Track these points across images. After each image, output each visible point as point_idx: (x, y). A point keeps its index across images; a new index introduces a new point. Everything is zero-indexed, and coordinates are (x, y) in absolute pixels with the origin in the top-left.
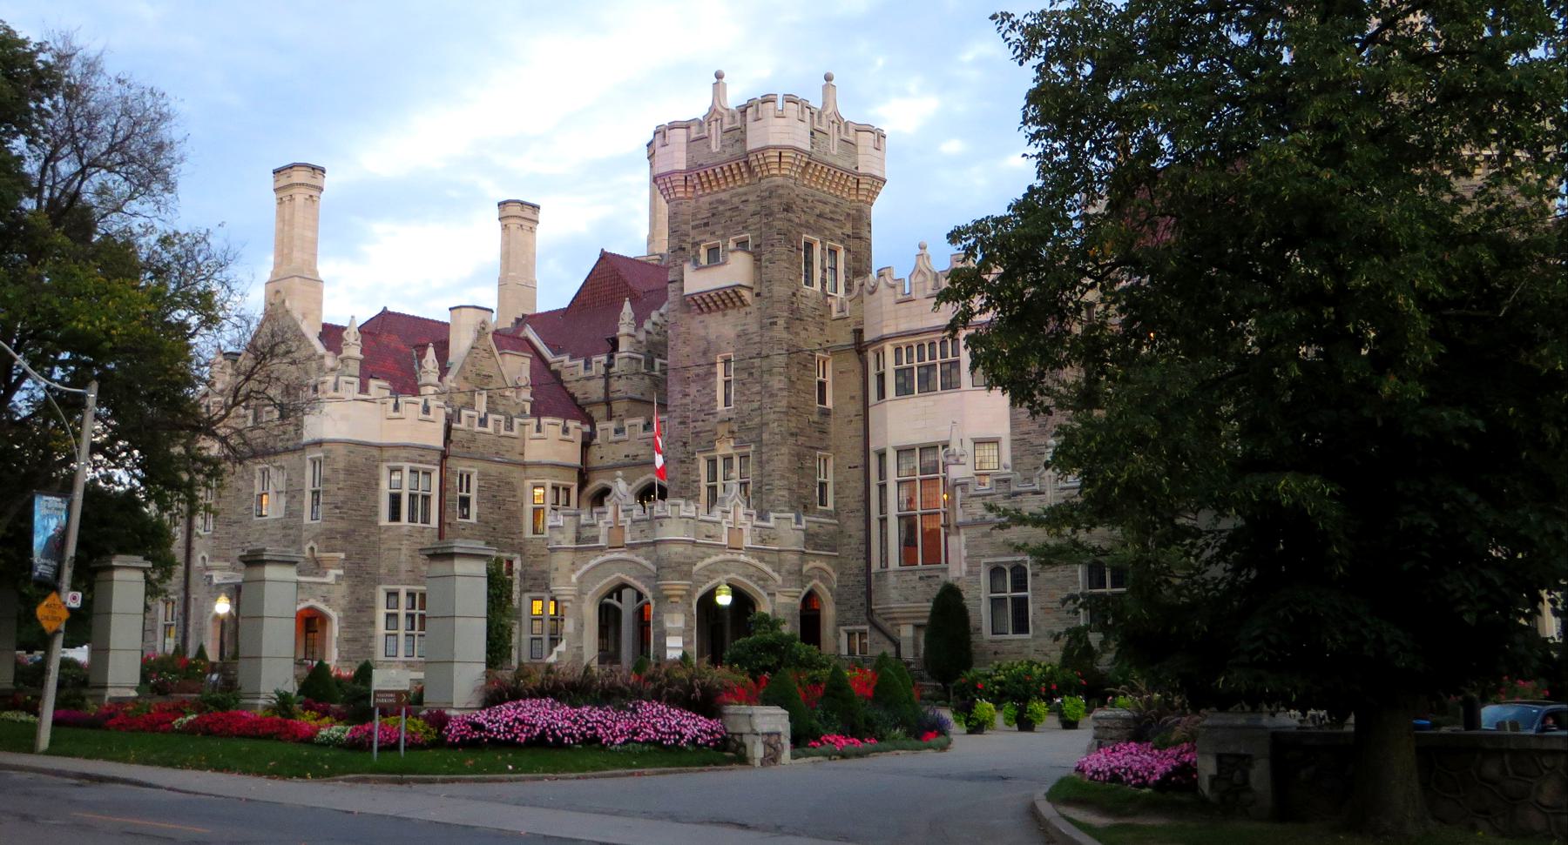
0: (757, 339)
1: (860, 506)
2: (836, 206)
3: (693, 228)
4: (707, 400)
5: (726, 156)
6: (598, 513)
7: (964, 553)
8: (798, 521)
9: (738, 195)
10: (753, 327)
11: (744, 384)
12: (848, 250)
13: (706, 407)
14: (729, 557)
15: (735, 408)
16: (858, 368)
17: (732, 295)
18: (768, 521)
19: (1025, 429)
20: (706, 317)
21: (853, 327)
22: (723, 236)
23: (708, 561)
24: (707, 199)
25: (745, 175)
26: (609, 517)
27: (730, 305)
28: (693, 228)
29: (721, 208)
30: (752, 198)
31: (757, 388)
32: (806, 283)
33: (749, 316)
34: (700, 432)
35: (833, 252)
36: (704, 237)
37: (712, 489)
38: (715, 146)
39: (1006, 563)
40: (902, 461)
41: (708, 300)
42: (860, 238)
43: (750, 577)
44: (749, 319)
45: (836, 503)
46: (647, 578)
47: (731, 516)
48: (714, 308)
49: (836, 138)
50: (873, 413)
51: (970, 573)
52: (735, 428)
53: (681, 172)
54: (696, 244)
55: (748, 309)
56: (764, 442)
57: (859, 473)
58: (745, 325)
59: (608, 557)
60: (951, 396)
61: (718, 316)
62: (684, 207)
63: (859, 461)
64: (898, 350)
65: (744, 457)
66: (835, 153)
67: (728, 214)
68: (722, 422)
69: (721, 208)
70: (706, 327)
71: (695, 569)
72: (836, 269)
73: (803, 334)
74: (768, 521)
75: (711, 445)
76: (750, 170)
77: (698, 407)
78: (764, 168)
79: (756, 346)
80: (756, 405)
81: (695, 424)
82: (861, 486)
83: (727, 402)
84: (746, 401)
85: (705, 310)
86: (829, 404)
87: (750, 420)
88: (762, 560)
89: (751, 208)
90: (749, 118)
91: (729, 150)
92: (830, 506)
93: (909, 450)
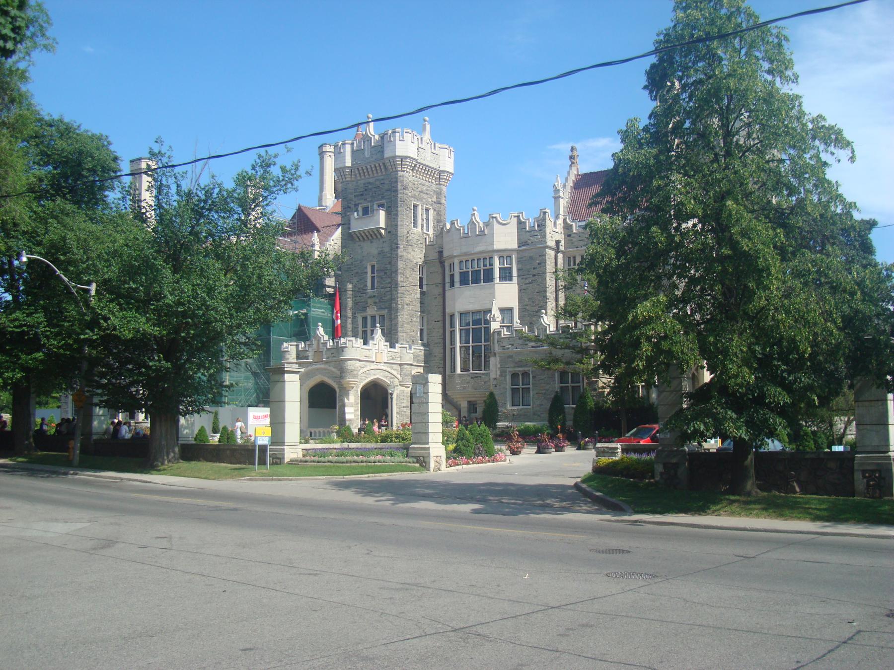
0: (389, 255)
1: (441, 341)
2: (428, 187)
3: (355, 196)
5: (373, 159)
7: (499, 366)
8: (410, 348)
9: (378, 180)
10: (387, 249)
12: (434, 210)
14: (376, 367)
16: (440, 270)
17: (376, 232)
18: (395, 348)
19: (525, 303)
21: (437, 250)
22: (371, 201)
23: (366, 369)
24: (363, 182)
25: (383, 170)
26: (315, 346)
27: (375, 237)
28: (355, 196)
29: (370, 187)
30: (387, 182)
31: (389, 280)
32: (414, 227)
35: (427, 210)
37: (365, 332)
38: (367, 154)
39: (519, 371)
40: (463, 318)
41: (363, 234)
42: (441, 204)
43: (386, 377)
45: (428, 339)
46: (335, 378)
47: (377, 346)
48: (366, 238)
49: (430, 151)
50: (448, 294)
51: (501, 376)
52: (377, 301)
53: (349, 167)
54: (356, 205)
55: (384, 240)
57: (440, 324)
59: (314, 367)
62: (350, 186)
63: (441, 318)
64: (461, 262)
65: (382, 316)
66: (428, 159)
67: (373, 190)
68: (370, 297)
69: (370, 187)
70: (362, 248)
71: (360, 373)
72: (427, 219)
73: (412, 253)
74: (395, 348)
75: (364, 309)
76: (386, 168)
78: (393, 167)
80: (388, 289)
82: (441, 331)
83: (373, 287)
85: (361, 239)
86: (425, 289)
88: (392, 368)
89: (386, 187)
90: (385, 140)
92: (425, 341)
93: (467, 313)
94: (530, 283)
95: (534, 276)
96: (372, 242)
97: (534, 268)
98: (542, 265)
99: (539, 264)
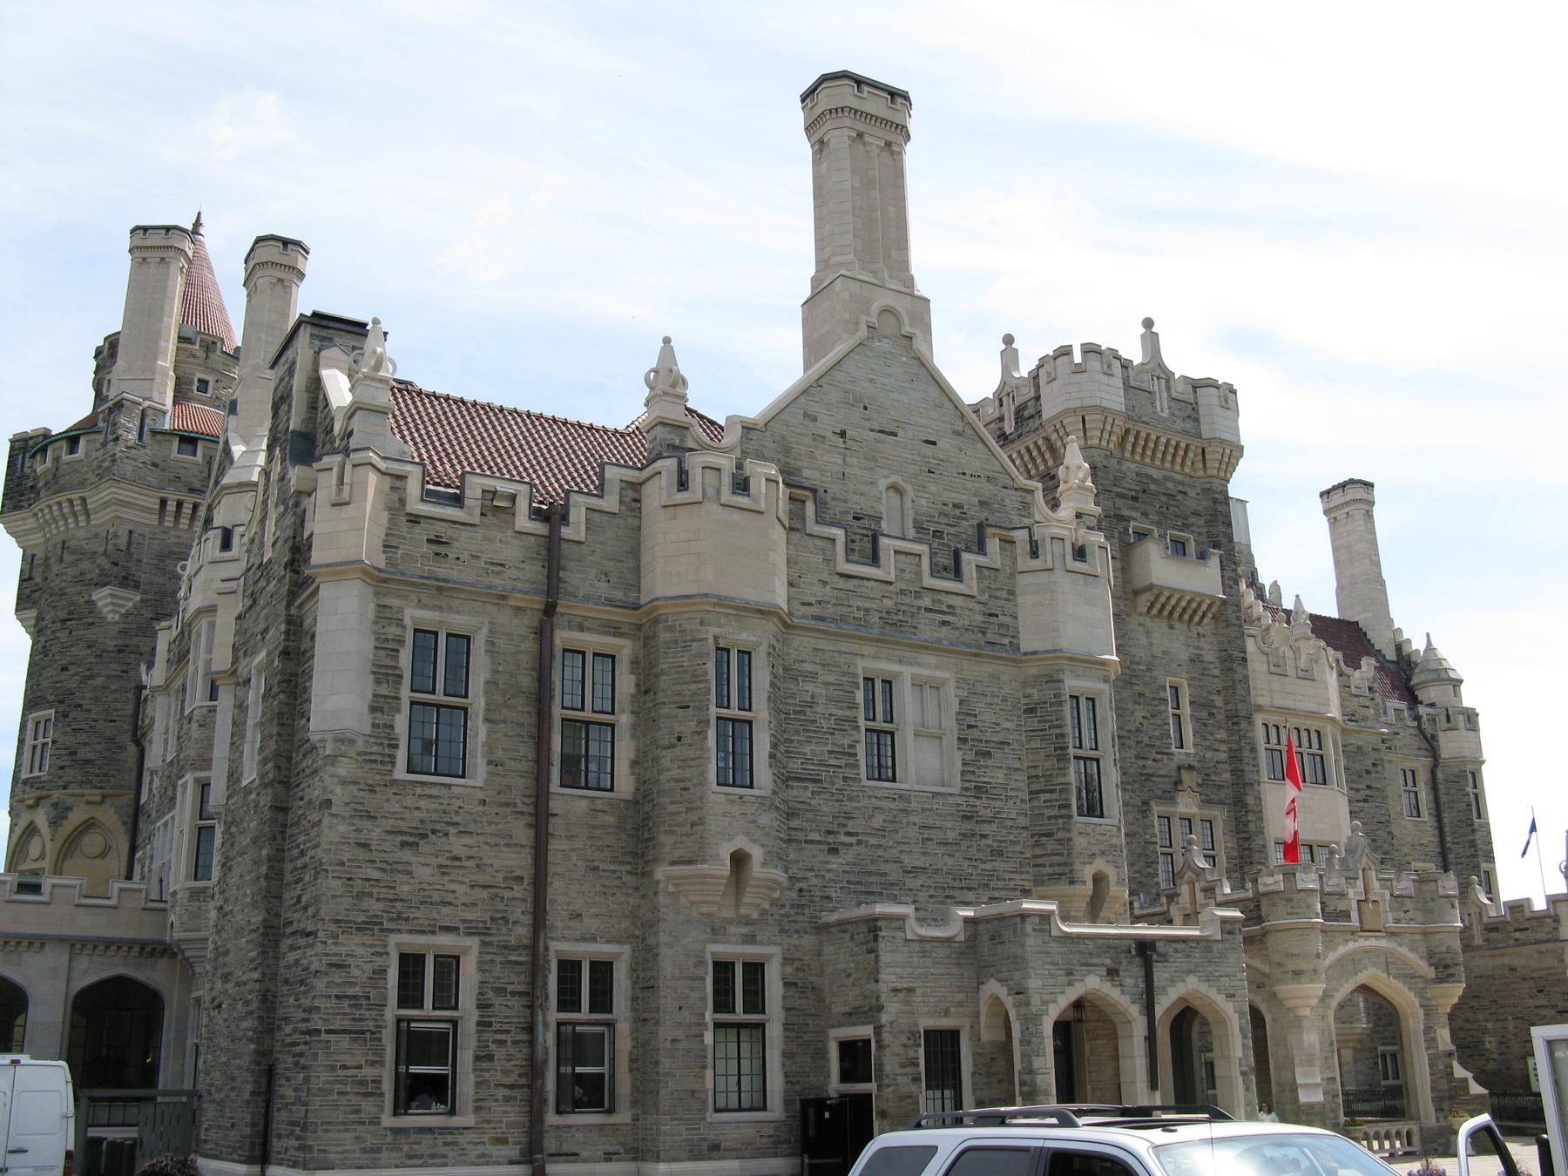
4: (1157, 733)
6: (1347, 878)
11: (1205, 725)
13: (1158, 743)
15: (1196, 754)
20: (1147, 621)
22: (1159, 524)
26: (1360, 883)
27: (1186, 617)
29: (1153, 487)
31: (1222, 735)
33: (1202, 640)
34: (1152, 775)
36: (1134, 514)
44: (1202, 643)
46: (1410, 978)
48: (1166, 613)
56: (1250, 808)
58: (1198, 648)
59: (1363, 943)
60: (1322, 791)
61: (1164, 624)
67: (1164, 499)
69: (1153, 487)
70: (1148, 634)
77: (1146, 740)
79: (1216, 680)
81: (1144, 762)
84: (1208, 748)
87: (1214, 773)
89: (1192, 505)
91: (1179, 425)
94: (1365, 801)
95: (1369, 787)
96: (1171, 627)
97: (1368, 772)
98: (1380, 768)
99: (1374, 765)
